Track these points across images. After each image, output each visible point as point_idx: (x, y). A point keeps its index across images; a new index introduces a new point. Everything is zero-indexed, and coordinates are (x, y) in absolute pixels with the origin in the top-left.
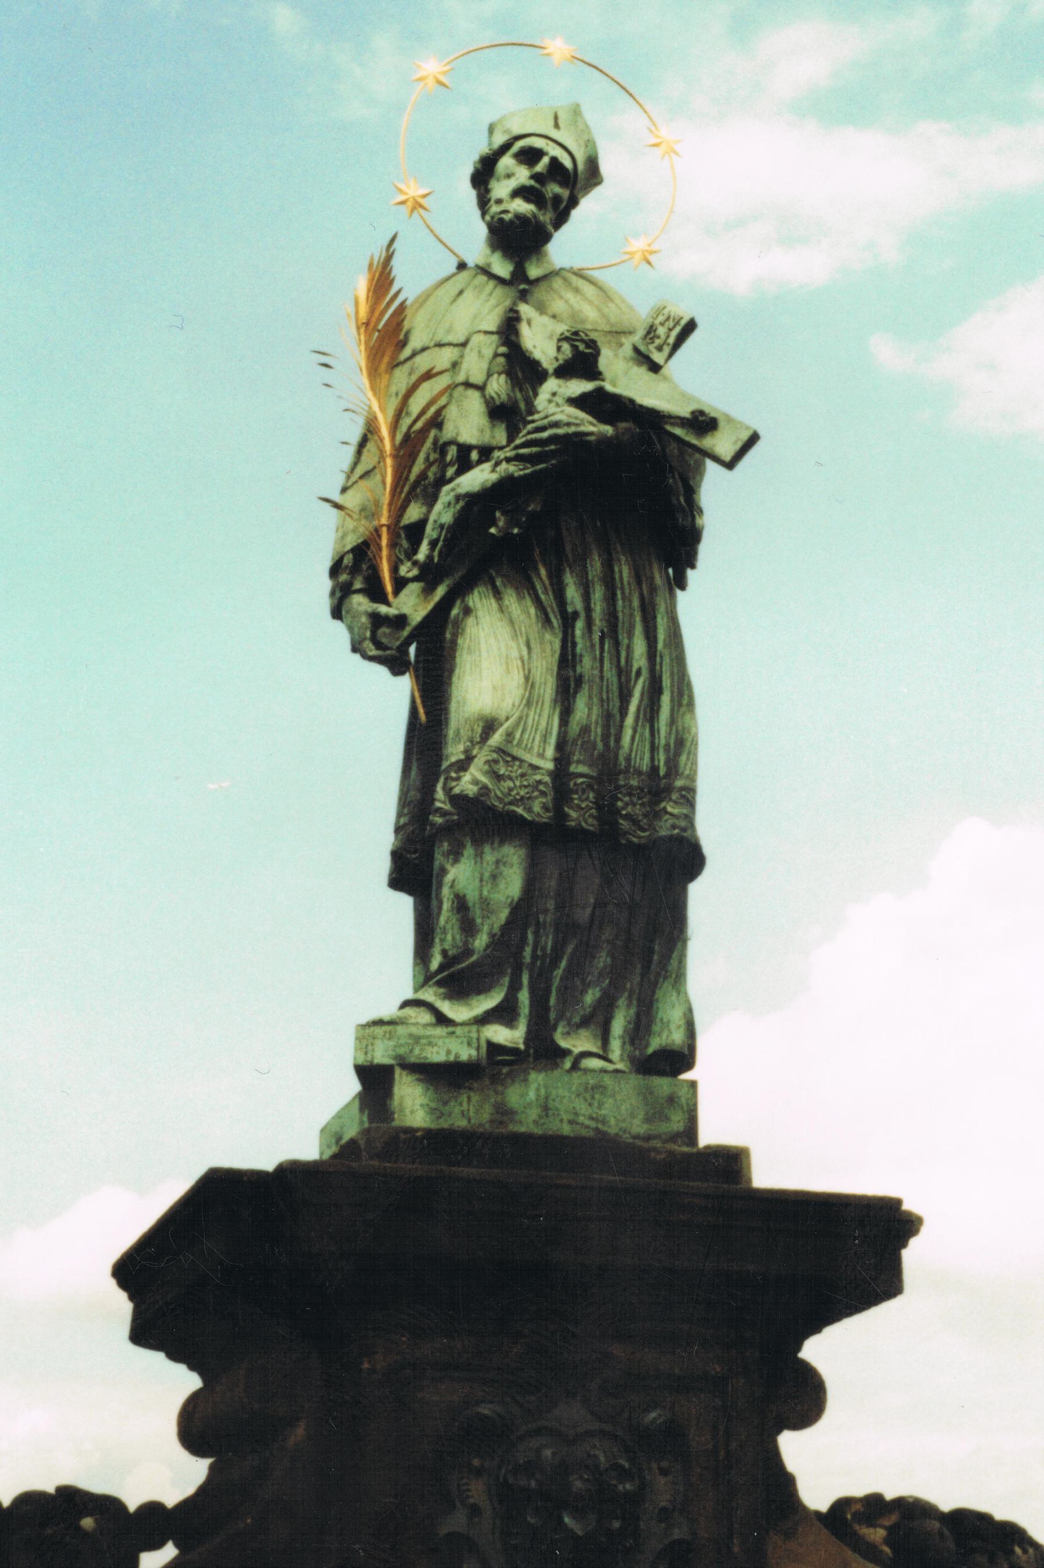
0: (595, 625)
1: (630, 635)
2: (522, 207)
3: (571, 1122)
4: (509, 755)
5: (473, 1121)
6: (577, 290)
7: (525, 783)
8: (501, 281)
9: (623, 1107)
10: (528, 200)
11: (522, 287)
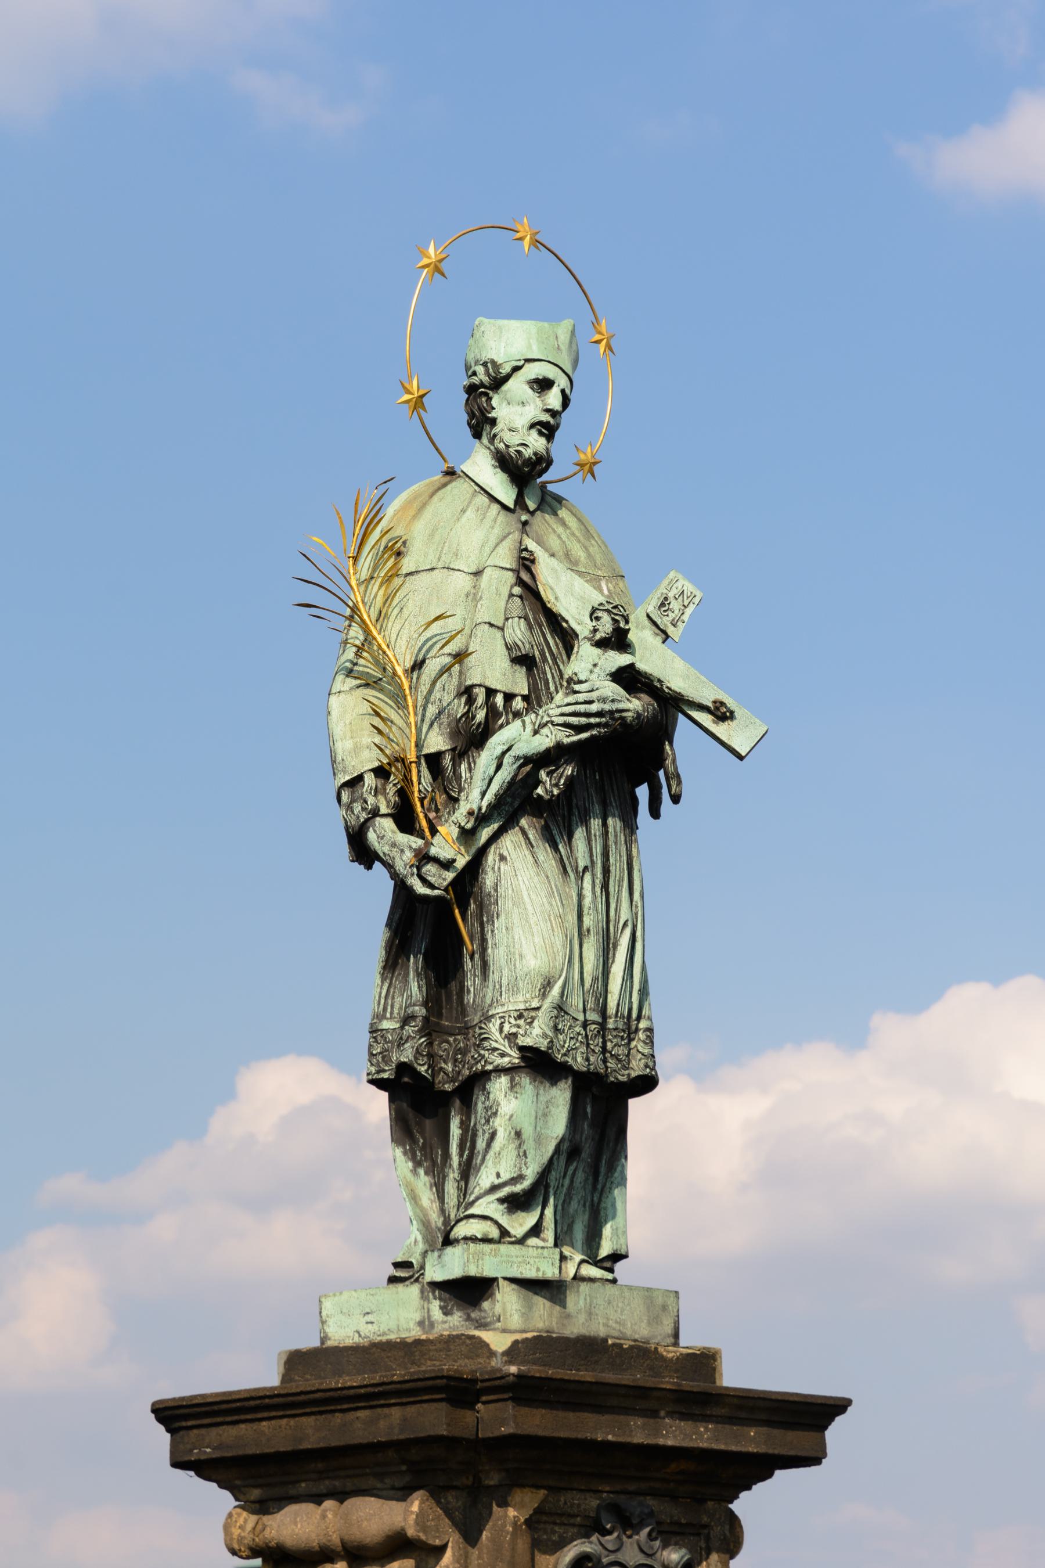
0: (597, 878)
1: (620, 886)
2: (536, 443)
3: (606, 1325)
4: (562, 1009)
5: (547, 1324)
6: (563, 523)
7: (572, 1036)
8: (504, 507)
9: (635, 1314)
10: (541, 433)
11: (524, 518)
